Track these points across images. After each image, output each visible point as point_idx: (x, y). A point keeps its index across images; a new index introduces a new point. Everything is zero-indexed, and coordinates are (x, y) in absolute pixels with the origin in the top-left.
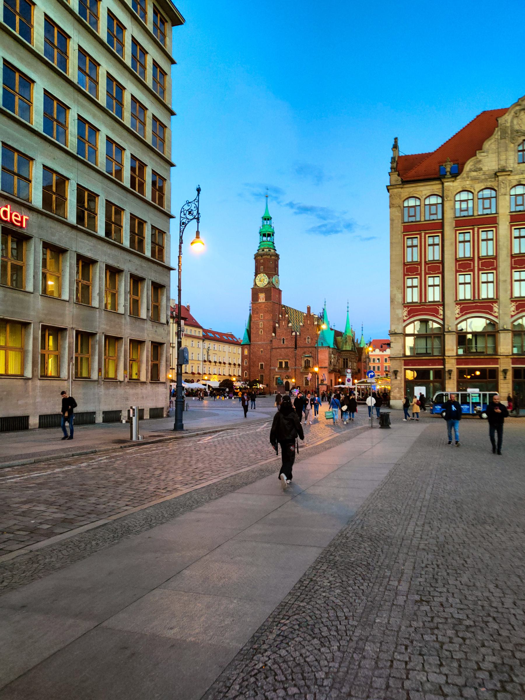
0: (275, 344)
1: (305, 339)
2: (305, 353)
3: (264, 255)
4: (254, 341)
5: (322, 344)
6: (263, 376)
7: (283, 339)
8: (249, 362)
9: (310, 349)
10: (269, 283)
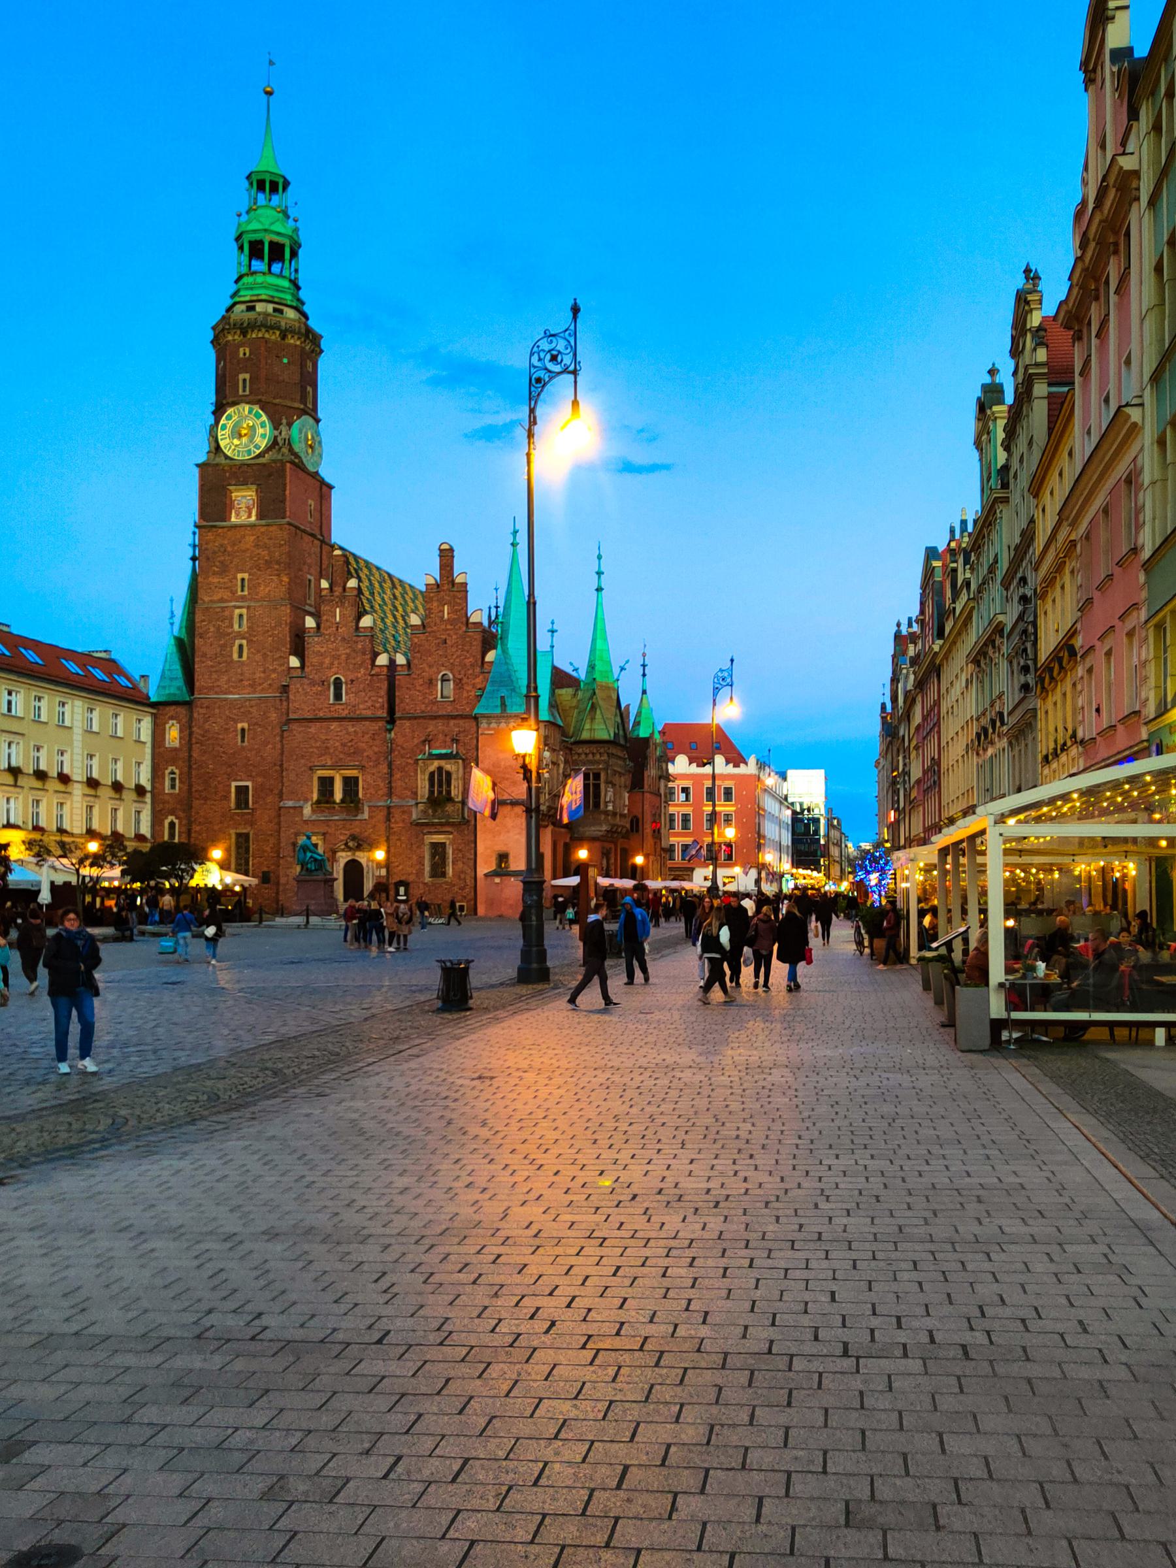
0: (302, 701)
1: (431, 683)
2: (428, 741)
3: (253, 326)
5: (503, 705)
6: (247, 835)
7: (338, 684)
8: (187, 778)
9: (454, 726)
10: (274, 444)
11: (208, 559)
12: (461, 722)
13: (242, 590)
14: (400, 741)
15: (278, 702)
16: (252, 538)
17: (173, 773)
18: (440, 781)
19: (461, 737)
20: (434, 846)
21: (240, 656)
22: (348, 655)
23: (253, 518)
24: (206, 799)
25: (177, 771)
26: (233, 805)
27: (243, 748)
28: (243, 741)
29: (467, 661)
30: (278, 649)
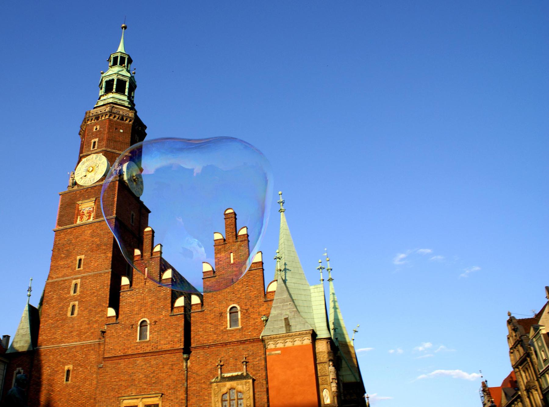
0: (114, 345)
1: (222, 315)
4: (48, 341)
9: (244, 351)
11: (59, 250)
12: (249, 346)
13: (79, 267)
14: (196, 368)
15: (97, 346)
16: (89, 232)
19: (250, 359)
21: (72, 314)
22: (153, 303)
23: (92, 219)
27: (67, 386)
28: (67, 380)
29: (253, 293)
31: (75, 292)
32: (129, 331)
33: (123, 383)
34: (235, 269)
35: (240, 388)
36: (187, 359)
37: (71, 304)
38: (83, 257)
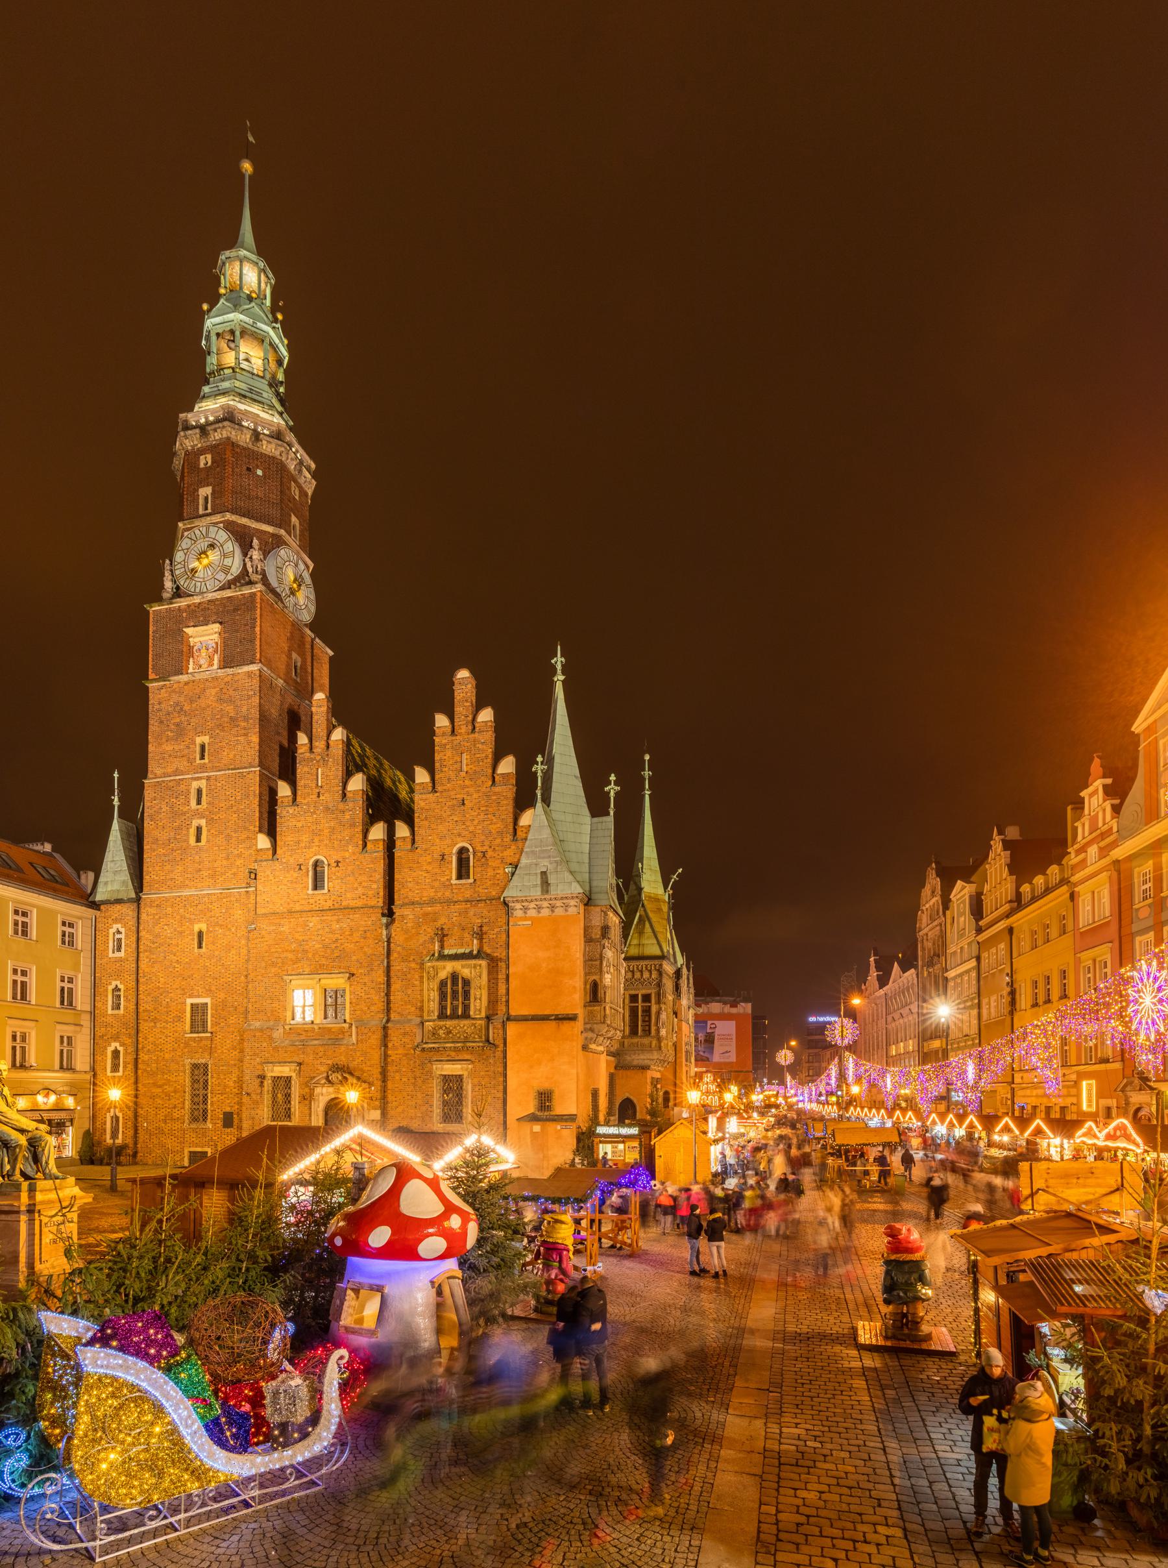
1: (443, 856)
6: (206, 1066)
13: (202, 757)
16: (213, 692)
17: (117, 989)
18: (455, 994)
20: (446, 1079)
21: (198, 840)
22: (333, 830)
24: (155, 1020)
25: (121, 987)
26: (188, 1027)
28: (200, 947)
29: (494, 827)
30: (246, 829)
31: (199, 802)
32: (295, 875)
33: (290, 956)
34: (467, 782)
35: (466, 972)
36: (388, 926)
37: (195, 823)
38: (206, 739)
